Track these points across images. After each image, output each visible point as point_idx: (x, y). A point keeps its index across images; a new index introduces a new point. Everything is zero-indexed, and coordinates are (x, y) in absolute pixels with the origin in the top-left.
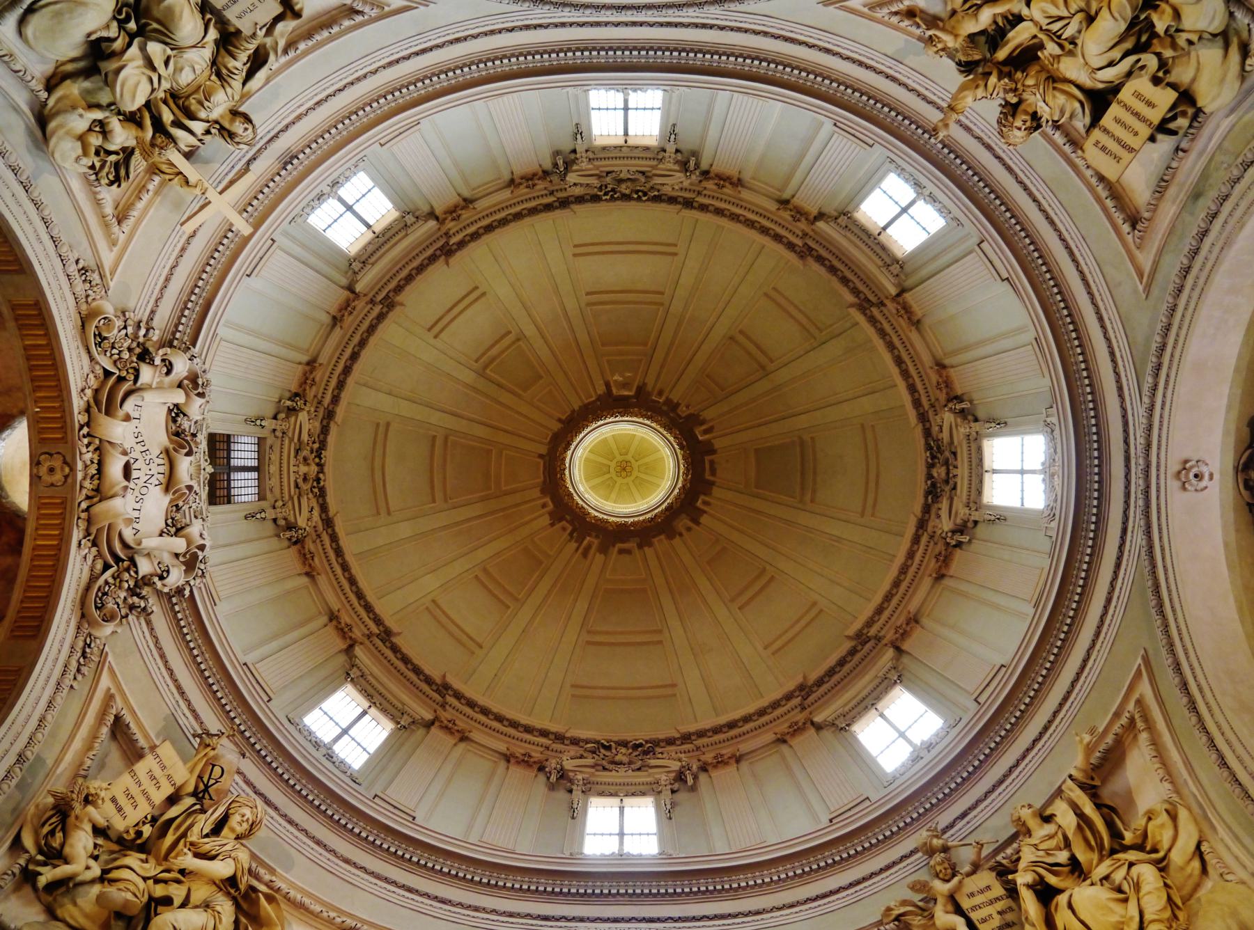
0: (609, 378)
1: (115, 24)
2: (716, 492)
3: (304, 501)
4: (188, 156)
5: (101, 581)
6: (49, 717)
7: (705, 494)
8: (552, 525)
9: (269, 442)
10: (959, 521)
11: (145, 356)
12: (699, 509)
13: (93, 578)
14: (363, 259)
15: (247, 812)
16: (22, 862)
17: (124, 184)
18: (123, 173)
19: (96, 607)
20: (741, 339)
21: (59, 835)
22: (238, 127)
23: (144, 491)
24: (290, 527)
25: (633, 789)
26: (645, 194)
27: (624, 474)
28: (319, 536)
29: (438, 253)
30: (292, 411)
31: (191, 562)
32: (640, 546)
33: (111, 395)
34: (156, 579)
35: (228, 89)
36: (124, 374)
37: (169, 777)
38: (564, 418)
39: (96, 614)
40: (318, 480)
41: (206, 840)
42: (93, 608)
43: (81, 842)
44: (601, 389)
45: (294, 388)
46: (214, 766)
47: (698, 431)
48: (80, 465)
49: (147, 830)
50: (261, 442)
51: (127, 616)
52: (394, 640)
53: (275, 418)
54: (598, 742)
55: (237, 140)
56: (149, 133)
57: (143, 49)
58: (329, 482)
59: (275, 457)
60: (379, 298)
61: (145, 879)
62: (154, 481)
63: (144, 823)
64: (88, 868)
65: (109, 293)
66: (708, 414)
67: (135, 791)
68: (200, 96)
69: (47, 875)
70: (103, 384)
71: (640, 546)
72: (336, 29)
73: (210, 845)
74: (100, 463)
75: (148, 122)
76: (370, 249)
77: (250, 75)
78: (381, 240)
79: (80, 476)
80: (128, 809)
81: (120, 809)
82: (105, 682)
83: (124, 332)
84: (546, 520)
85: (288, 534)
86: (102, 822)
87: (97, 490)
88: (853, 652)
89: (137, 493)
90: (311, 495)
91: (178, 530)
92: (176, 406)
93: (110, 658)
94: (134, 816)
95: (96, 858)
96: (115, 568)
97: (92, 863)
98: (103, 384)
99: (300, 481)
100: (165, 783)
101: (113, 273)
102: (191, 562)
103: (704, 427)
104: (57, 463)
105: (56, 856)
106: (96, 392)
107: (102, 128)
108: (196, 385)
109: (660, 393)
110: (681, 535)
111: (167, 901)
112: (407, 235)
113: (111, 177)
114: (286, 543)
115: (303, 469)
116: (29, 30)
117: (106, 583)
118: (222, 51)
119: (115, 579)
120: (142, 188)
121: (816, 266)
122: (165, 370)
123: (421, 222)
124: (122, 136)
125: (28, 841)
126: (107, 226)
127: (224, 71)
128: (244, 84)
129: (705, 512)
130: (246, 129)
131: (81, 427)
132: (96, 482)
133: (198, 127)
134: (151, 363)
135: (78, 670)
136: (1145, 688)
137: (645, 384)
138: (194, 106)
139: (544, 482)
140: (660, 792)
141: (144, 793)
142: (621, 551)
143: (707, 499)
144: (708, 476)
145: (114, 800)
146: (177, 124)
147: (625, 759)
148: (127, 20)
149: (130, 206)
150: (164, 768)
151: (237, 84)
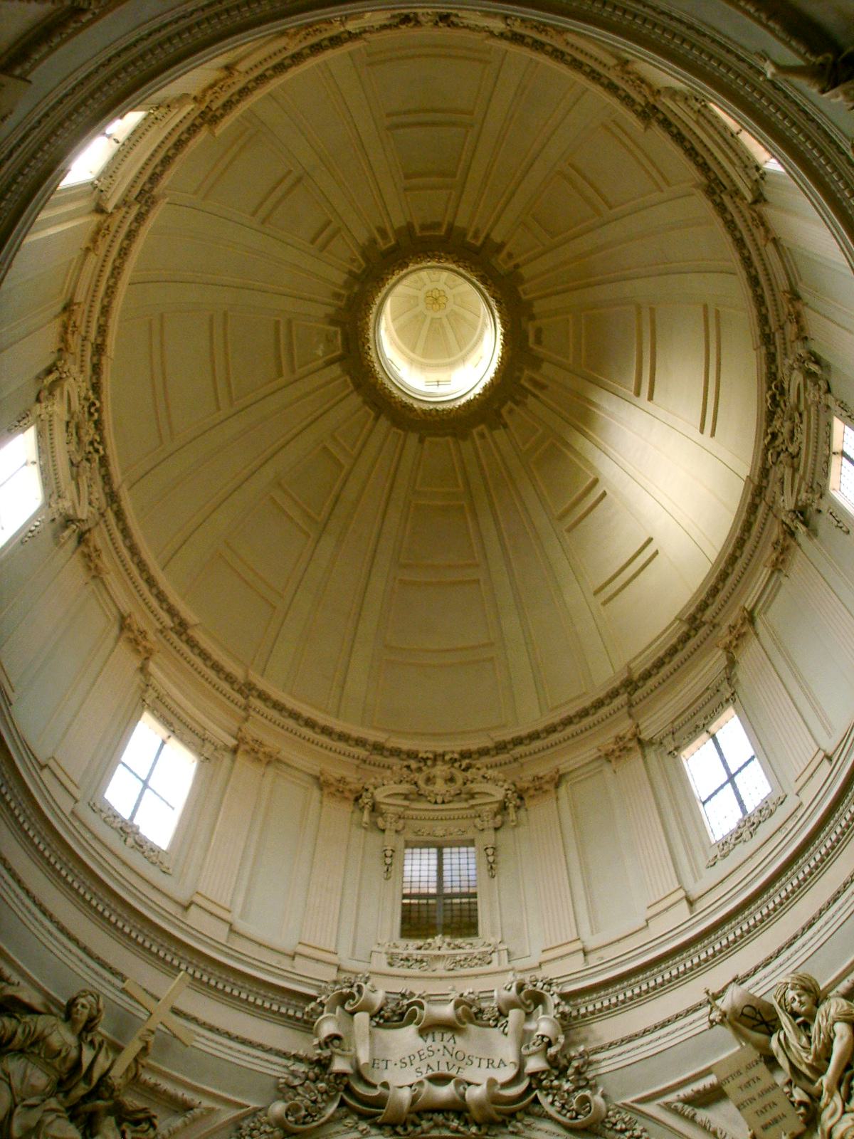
0: (320, 362)
2: (461, 222)
3: (476, 787)
4: (118, 1049)
5: (552, 1111)
7: (465, 236)
8: (505, 426)
9: (411, 837)
11: (323, 1064)
12: (484, 244)
14: (199, 741)
17: (153, 1112)
18: (141, 1116)
19: (576, 1118)
20: (263, 212)
22: (82, 1015)
23: (460, 1055)
24: (503, 807)
25: (822, 435)
27: (442, 300)
28: (516, 760)
29: (184, 637)
30: (375, 808)
31: (532, 1000)
32: (532, 317)
34: (552, 1051)
36: (342, 1087)
37: (749, 1067)
38: (373, 414)
40: (453, 761)
41: (813, 1047)
44: (336, 370)
45: (347, 807)
46: (742, 1014)
49: (798, 1095)
50: (408, 845)
51: (587, 1080)
52: (636, 676)
54: (767, 449)
55: (95, 1012)
56: (100, 1103)
58: (454, 746)
60: (242, 701)
61: (844, 1112)
62: (450, 1045)
63: (792, 1095)
66: (362, 237)
67: (758, 1105)
68: (57, 1062)
70: (353, 1111)
71: (532, 317)
73: (816, 1045)
75: (89, 1107)
76: (189, 736)
77: (30, 1010)
78: (177, 725)
80: (775, 1112)
81: (775, 1121)
82: (650, 1108)
83: (300, 1090)
84: (500, 434)
85: (511, 810)
89: (462, 1064)
90: (469, 774)
92: (372, 1017)
93: (628, 1100)
94: (784, 1107)
96: (537, 1092)
98: (353, 1111)
100: (754, 1072)
101: (241, 1106)
102: (532, 1000)
103: (379, 240)
106: (363, 1116)
108: (351, 996)
109: (337, 296)
110: (517, 266)
112: (168, 695)
114: (522, 813)
115: (440, 786)
117: (552, 1103)
118: (10, 1047)
119: (547, 1095)
120: (154, 1090)
121: (165, 182)
122: (336, 1042)
123: (153, 681)
126: (194, 1120)
128: (39, 1013)
129: (487, 237)
130: (83, 1006)
133: (87, 1055)
137: (327, 316)
138: (68, 1064)
139: (454, 435)
141: (762, 1094)
142: (538, 341)
143: (471, 234)
144: (442, 232)
145: (765, 1127)
147: (788, 425)
150: (739, 1073)
151: (41, 1023)
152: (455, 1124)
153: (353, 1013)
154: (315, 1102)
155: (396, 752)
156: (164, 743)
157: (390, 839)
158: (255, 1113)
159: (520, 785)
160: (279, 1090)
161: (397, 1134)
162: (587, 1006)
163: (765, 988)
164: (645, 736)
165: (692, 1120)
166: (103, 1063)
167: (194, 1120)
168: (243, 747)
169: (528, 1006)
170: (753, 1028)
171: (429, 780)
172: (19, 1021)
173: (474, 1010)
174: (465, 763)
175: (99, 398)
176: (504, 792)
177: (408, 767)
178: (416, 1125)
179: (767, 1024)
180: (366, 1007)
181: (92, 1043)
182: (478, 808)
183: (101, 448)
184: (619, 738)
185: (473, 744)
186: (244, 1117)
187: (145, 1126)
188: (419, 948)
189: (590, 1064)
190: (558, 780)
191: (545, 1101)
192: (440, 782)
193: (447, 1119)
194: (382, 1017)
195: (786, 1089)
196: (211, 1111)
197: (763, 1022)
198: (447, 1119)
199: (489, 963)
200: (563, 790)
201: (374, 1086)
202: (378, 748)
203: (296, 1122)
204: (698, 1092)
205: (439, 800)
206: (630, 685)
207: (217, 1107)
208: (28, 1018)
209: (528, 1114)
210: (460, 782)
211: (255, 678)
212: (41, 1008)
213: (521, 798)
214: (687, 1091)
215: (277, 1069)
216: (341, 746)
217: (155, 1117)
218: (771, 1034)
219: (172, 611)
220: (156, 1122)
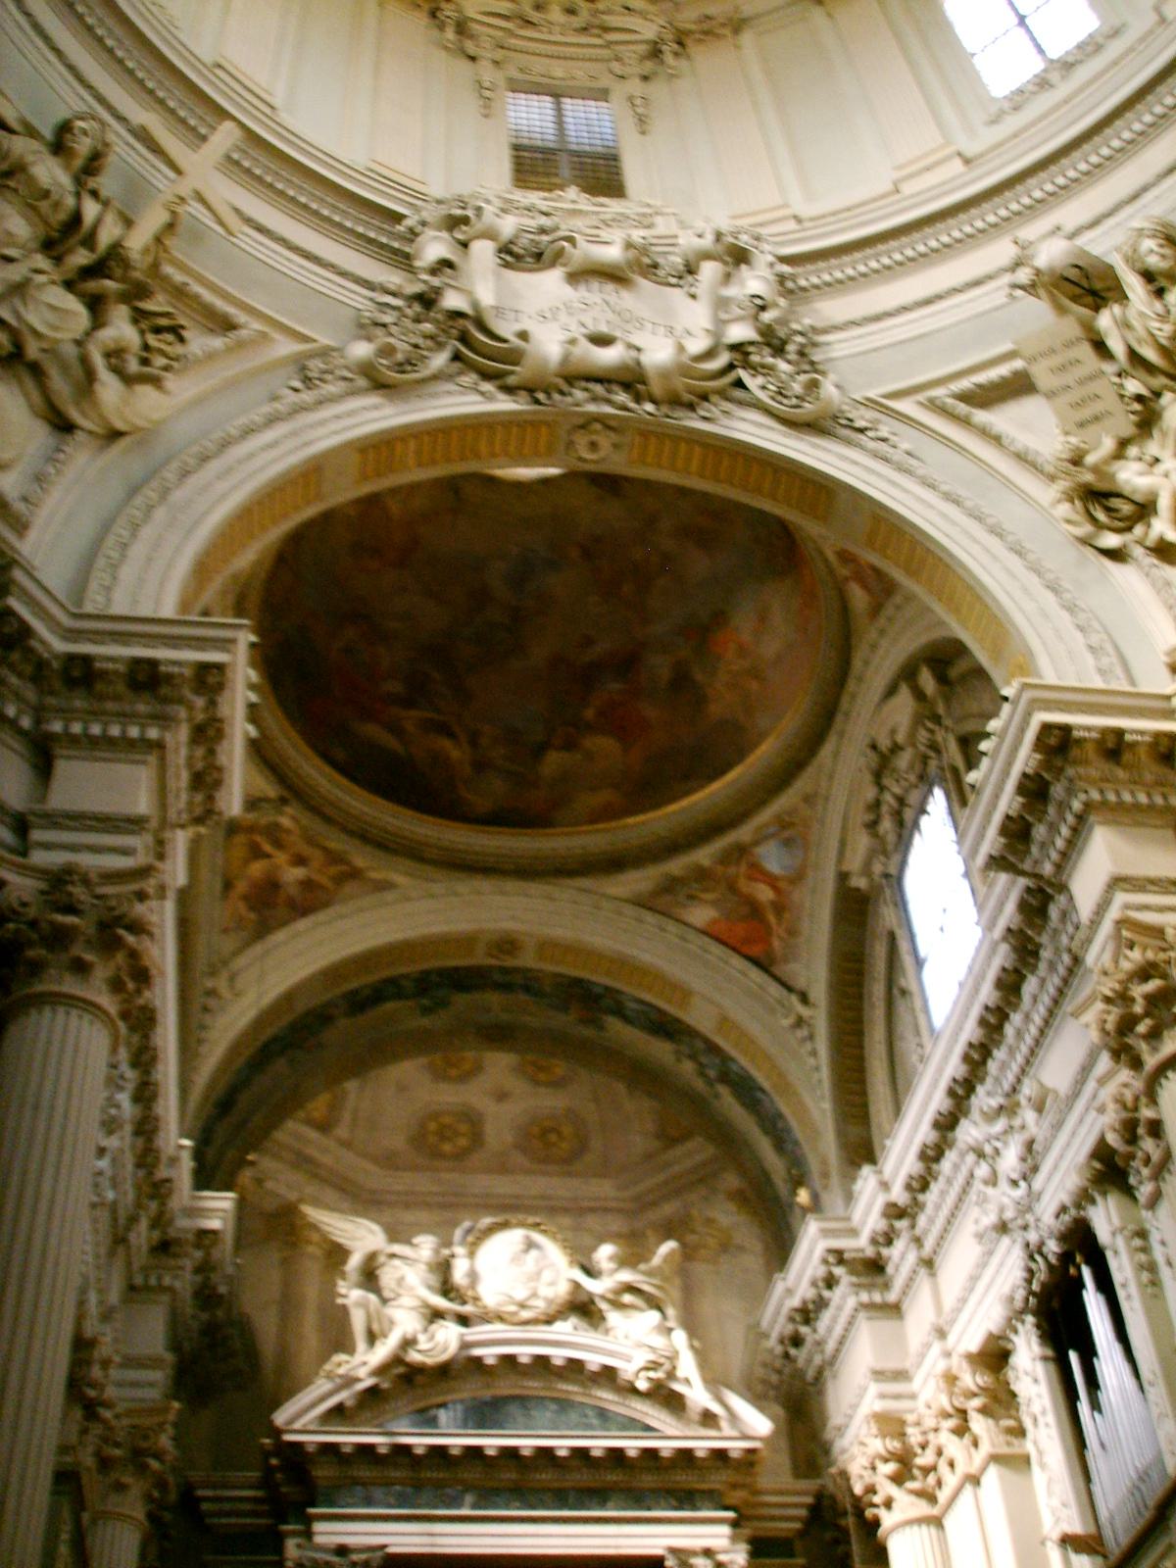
4: (128, 223)
6: (944, 488)
11: (427, 300)
17: (183, 322)
18: (164, 322)
21: (1115, 503)
22: (83, 146)
24: (655, 52)
30: (462, 28)
33: (478, 348)
34: (767, 317)
37: (1069, 345)
45: (421, 20)
48: (592, 408)
49: (1133, 386)
50: (515, 87)
51: (812, 363)
53: (473, 59)
56: (109, 284)
59: (538, 65)
64: (1166, 475)
65: (332, 343)
67: (1075, 395)
68: (44, 206)
74: (589, 379)
79: (608, 410)
81: (1097, 418)
82: (904, 406)
85: (669, 59)
86: (1108, 445)
87: (627, 386)
89: (629, 327)
93: (872, 394)
94: (1110, 402)
95: (1157, 460)
97: (1160, 468)
99: (577, 21)
101: (306, 339)
104: (581, 440)
106: (487, 376)
108: (465, 220)
120: (180, 293)
124: (121, 328)
125: (1111, 540)
126: (241, 344)
130: (85, 133)
131: (537, 402)
133: (90, 210)
138: (63, 216)
141: (1081, 382)
146: (90, 241)
152: (622, 397)
157: (488, 73)
158: (324, 353)
161: (537, 402)
162: (808, 277)
163: (1106, 246)
165: (965, 422)
170: (1075, 299)
173: (646, 260)
178: (562, 393)
179: (1094, 293)
180: (489, 234)
182: (617, 48)
186: (311, 355)
187: (170, 337)
189: (815, 345)
191: (753, 383)
193: (609, 391)
195: (1116, 380)
196: (264, 335)
198: (609, 391)
203: (388, 368)
204: (980, 386)
213: (680, 43)
214: (965, 384)
215: (359, 300)
217: (182, 327)
218: (1097, 309)
220: (185, 334)
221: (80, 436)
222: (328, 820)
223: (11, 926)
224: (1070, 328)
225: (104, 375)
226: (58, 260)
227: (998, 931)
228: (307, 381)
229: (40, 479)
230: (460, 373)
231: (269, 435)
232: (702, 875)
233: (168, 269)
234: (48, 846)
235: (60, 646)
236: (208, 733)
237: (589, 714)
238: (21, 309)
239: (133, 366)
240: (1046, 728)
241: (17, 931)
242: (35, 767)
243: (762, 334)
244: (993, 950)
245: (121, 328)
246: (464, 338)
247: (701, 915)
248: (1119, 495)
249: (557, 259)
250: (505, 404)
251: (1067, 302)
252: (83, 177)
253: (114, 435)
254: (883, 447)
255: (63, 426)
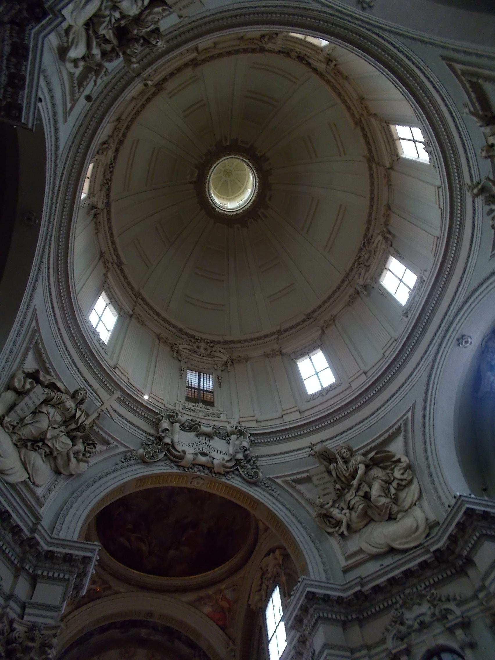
1: (40, 450)
3: (216, 354)
4: (88, 415)
6: (288, 506)
10: (323, 60)
11: (160, 439)
13: (241, 476)
15: (343, 450)
16: (337, 535)
19: (252, 478)
21: (331, 520)
22: (80, 397)
23: (211, 447)
24: (226, 364)
26: (112, 164)
28: (230, 348)
29: (120, 268)
35: (65, 400)
36: (166, 449)
39: (254, 479)
42: (253, 481)
43: (336, 512)
45: (169, 349)
46: (322, 454)
47: (224, 143)
48: (199, 473)
49: (338, 486)
51: (257, 466)
53: (180, 361)
54: (355, 262)
56: (79, 433)
57: (49, 440)
58: (210, 338)
60: (135, 299)
61: (355, 496)
63: (335, 486)
64: (345, 514)
65: (134, 449)
69: (343, 528)
72: (43, 351)
73: (351, 469)
74: (199, 465)
75: (74, 434)
77: (59, 390)
81: (328, 494)
82: (279, 481)
85: (229, 366)
87: (209, 468)
88: (363, 129)
89: (211, 451)
90: (214, 349)
91: (228, 436)
92: (180, 426)
93: (271, 476)
94: (331, 490)
95: (342, 509)
97: (344, 512)
101: (127, 447)
103: (224, 142)
105: (338, 524)
106: (172, 461)
107: (76, 453)
108: (173, 416)
111: (366, 493)
113: (92, 446)
115: (202, 350)
116: (40, 483)
117: (243, 472)
118: (49, 403)
123: (108, 280)
125: (330, 530)
126: (110, 448)
127: (58, 402)
128: (63, 393)
129: (264, 154)
130: (81, 394)
131: (185, 470)
132: (206, 468)
133: (78, 413)
134: (164, 437)
135: (273, 490)
136: (458, 67)
138: (71, 415)
140: (389, 251)
145: (324, 495)
147: (368, 254)
148: (38, 446)
149: (103, 438)
150: (318, 474)
151: (64, 397)
152: (207, 472)
153: (173, 423)
154: (156, 452)
155: (187, 334)
156: (107, 305)
158: (131, 451)
159: (234, 357)
160: (142, 444)
161: (185, 470)
164: (284, 351)
165: (294, 488)
166: (83, 418)
167: (110, 448)
168: (134, 316)
169: (238, 435)
170: (324, 460)
171: (198, 347)
172: (55, 394)
173: (218, 432)
174: (212, 345)
175: (115, 162)
176: (226, 358)
177: (190, 340)
179: (330, 460)
180: (178, 421)
181: (80, 409)
183: (109, 183)
184: (273, 350)
185: (216, 339)
187: (92, 446)
188: (193, 406)
190: (247, 359)
192: (202, 349)
194: (183, 427)
195: (333, 484)
196: (117, 446)
197: (329, 459)
199: (220, 417)
200: (249, 362)
201: (179, 452)
202: (181, 331)
204: (298, 479)
205: (202, 355)
206: (280, 332)
207: (119, 446)
208: (59, 393)
209: (233, 474)
210: (209, 351)
211: (142, 291)
212: (63, 391)
213: (232, 362)
214: (294, 477)
216: (168, 326)
218: (330, 464)
219: (118, 256)
220: (96, 446)
221: (62, 476)
222: (105, 570)
223: (14, 645)
224: (322, 468)
225: (73, 460)
226: (67, 426)
227: (293, 645)
228: (125, 459)
229: (49, 490)
230: (166, 460)
231: (112, 476)
232: (209, 597)
233: (95, 427)
234: (30, 615)
235: (46, 548)
236: (82, 575)
237: (184, 539)
238: (55, 443)
239: (81, 457)
240: (308, 592)
241: (16, 646)
242: (30, 584)
243: (244, 457)
244: (290, 651)
245: (80, 446)
246: (168, 450)
247: (207, 610)
248: (332, 518)
249: (195, 429)
250: (176, 470)
251: (322, 460)
252: (78, 405)
253: (71, 475)
254: (273, 492)
255: (58, 472)
